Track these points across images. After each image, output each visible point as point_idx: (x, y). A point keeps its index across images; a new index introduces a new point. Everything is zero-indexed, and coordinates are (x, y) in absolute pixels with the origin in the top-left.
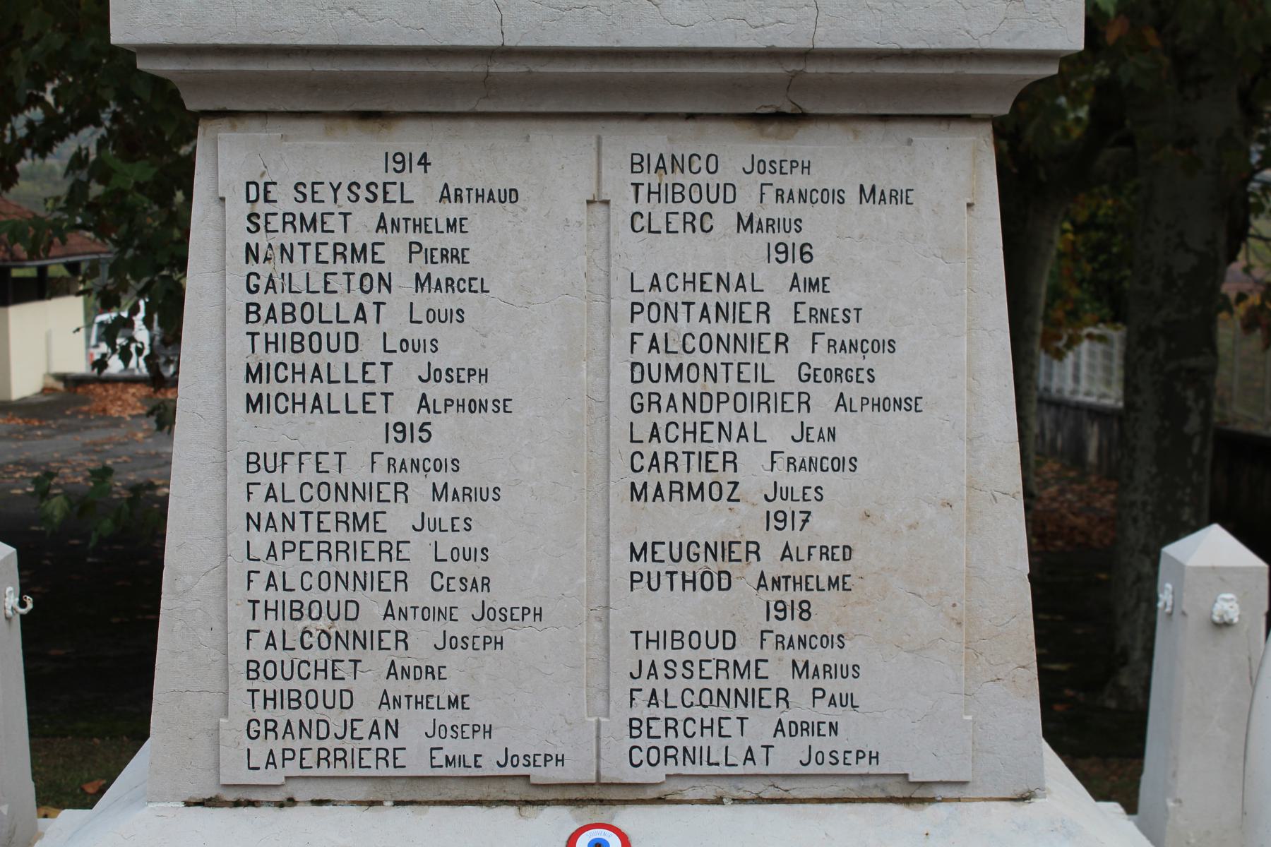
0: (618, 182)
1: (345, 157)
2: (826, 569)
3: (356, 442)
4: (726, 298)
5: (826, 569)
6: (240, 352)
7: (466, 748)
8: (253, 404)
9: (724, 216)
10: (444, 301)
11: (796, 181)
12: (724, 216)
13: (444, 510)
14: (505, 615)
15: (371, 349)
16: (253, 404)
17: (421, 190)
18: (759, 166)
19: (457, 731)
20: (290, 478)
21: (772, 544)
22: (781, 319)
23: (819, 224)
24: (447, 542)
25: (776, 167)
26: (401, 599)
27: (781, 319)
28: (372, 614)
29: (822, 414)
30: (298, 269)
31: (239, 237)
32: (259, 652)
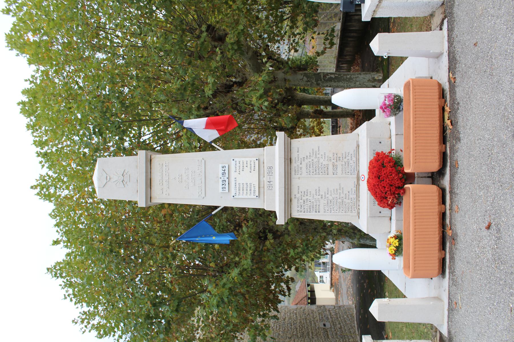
0: (297, 176)
1: (295, 203)
2: (335, 155)
3: (323, 202)
4: (308, 165)
5: (335, 155)
6: (314, 213)
7: (353, 191)
8: (319, 212)
9: (300, 166)
10: (309, 193)
11: (297, 159)
12: (300, 166)
13: (329, 193)
14: (340, 187)
15: (314, 200)
16: (319, 212)
17: (298, 196)
18: (295, 162)
19: (352, 192)
20: (326, 209)
21: (333, 161)
22: (310, 160)
23: (301, 156)
24: (333, 193)
25: (295, 161)
26: (338, 198)
27: (310, 160)
28: (340, 200)
29: (320, 156)
30: (306, 208)
31: (303, 213)
32: (343, 212)
